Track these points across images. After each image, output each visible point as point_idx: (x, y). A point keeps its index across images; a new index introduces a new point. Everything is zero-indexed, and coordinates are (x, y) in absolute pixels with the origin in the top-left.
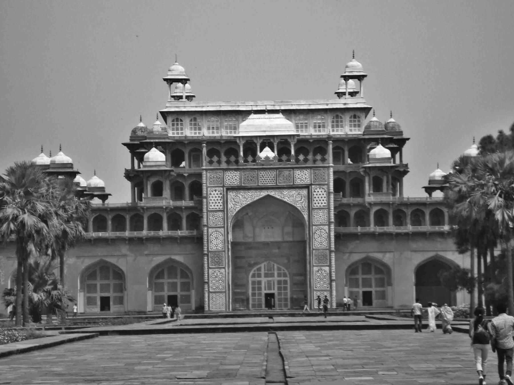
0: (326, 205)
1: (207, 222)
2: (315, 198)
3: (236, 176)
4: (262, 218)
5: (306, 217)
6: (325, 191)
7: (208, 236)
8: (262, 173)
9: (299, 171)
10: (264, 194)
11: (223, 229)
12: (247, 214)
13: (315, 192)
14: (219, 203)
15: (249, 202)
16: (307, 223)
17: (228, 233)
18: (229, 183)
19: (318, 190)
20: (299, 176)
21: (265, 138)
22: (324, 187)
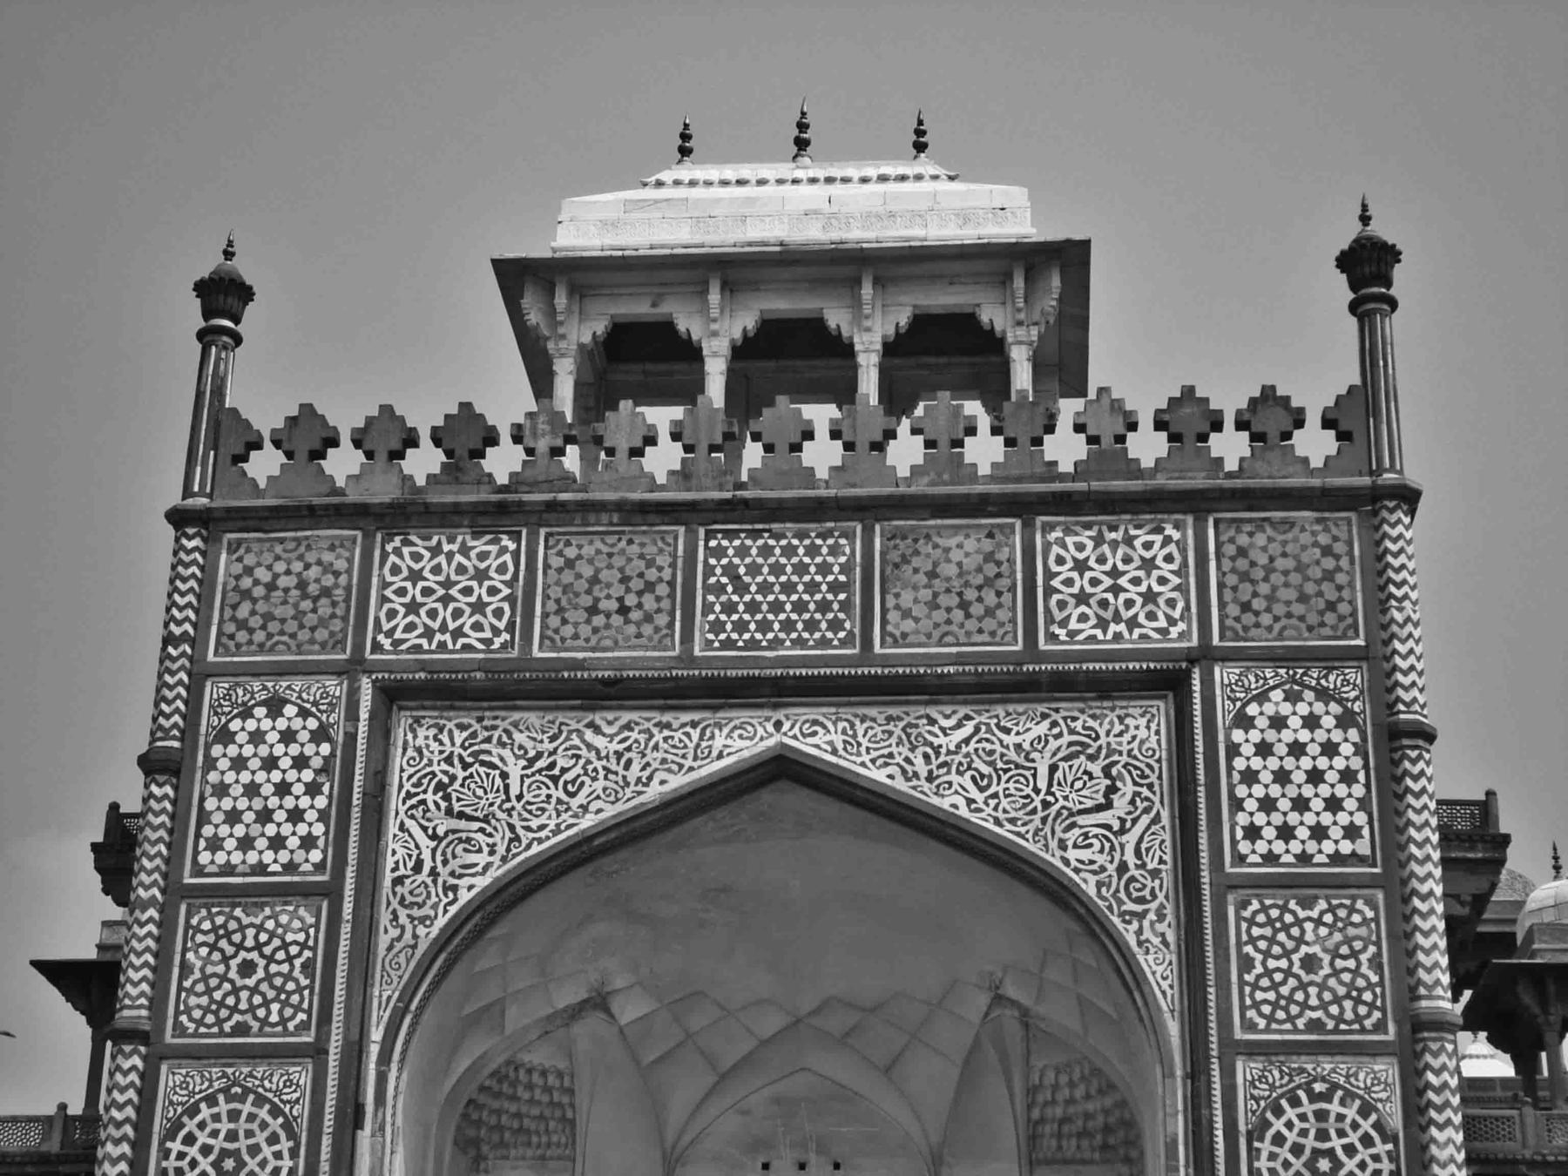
0: (1363, 847)
1: (157, 1004)
2: (1250, 777)
3: (481, 576)
4: (746, 1062)
5: (1159, 969)
6: (1345, 721)
7: (140, 1145)
8: (737, 549)
9: (1086, 537)
10: (740, 740)
11: (302, 1075)
12: (599, 1002)
13: (1245, 722)
14: (296, 816)
15: (587, 822)
16: (1173, 1028)
17: (351, 1116)
18: (413, 638)
19: (1278, 702)
20: (1081, 583)
21: (783, 304)
22: (1333, 680)
